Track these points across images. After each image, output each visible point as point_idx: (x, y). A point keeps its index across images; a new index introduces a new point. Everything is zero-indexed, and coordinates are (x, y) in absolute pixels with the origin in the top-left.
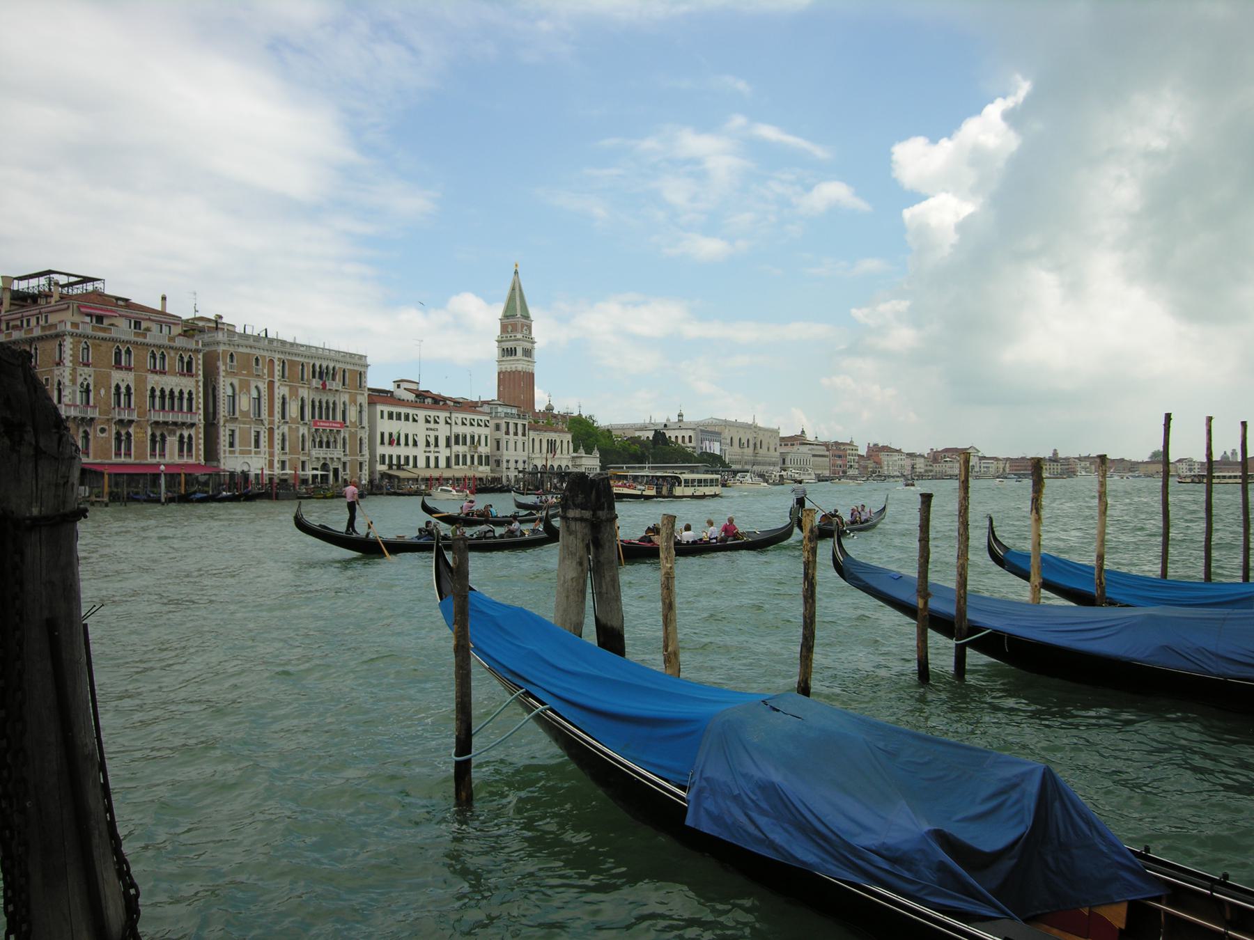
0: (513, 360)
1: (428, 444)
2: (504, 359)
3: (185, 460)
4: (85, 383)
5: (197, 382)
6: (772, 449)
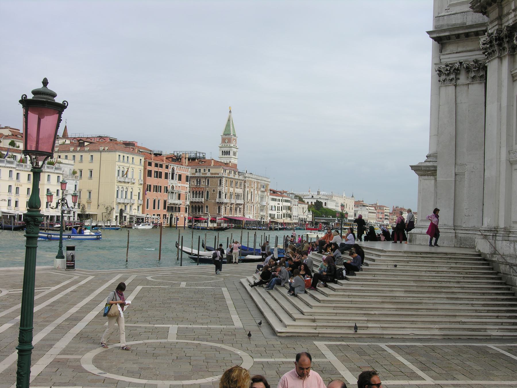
1: (278, 210)
2: (223, 156)
3: (240, 216)
6: (351, 208)
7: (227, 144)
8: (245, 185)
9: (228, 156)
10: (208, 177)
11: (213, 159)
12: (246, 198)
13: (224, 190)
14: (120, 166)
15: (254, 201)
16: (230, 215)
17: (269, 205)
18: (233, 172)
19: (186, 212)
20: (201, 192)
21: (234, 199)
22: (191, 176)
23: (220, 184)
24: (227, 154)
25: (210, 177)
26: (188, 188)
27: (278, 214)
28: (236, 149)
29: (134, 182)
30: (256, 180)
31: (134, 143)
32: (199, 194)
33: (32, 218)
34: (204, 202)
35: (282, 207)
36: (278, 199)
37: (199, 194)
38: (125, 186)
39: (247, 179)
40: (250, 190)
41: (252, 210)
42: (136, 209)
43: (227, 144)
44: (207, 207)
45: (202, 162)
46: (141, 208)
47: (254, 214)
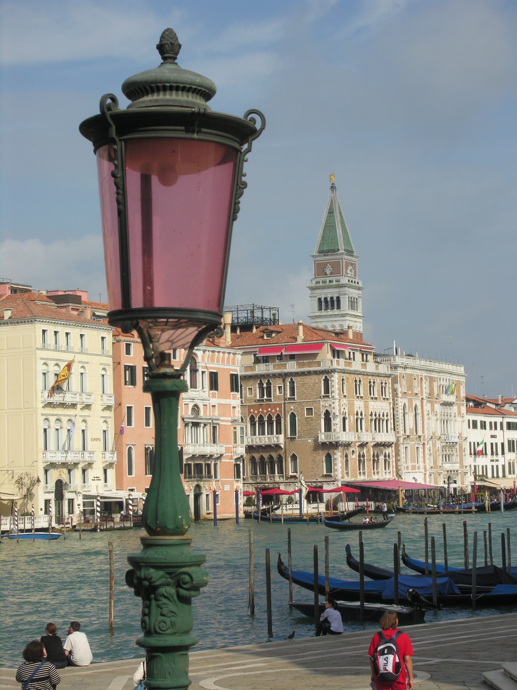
0: (335, 316)
1: (492, 454)
2: (323, 313)
4: (344, 412)
5: (390, 403)
7: (331, 279)
8: (395, 390)
9: (336, 312)
10: (291, 374)
11: (299, 324)
12: (401, 425)
13: (337, 408)
14: (49, 362)
15: (423, 432)
16: (361, 478)
17: (468, 440)
18: (358, 355)
19: (238, 476)
20: (274, 419)
21: (367, 431)
22: (244, 373)
23: (327, 390)
24: (333, 305)
25: (297, 374)
26: (238, 409)
27: (495, 464)
28: (356, 291)
29: (88, 402)
30: (424, 374)
31: (78, 293)
32: (270, 423)
33: (170, 574)
34: (285, 445)
35: (503, 444)
36: (491, 423)
37: (270, 423)
38: (64, 415)
39: (400, 371)
40: (410, 401)
41: (421, 459)
42: (98, 479)
43: (331, 279)
44: (294, 458)
45: (272, 332)
46: (111, 473)
47: (426, 470)
